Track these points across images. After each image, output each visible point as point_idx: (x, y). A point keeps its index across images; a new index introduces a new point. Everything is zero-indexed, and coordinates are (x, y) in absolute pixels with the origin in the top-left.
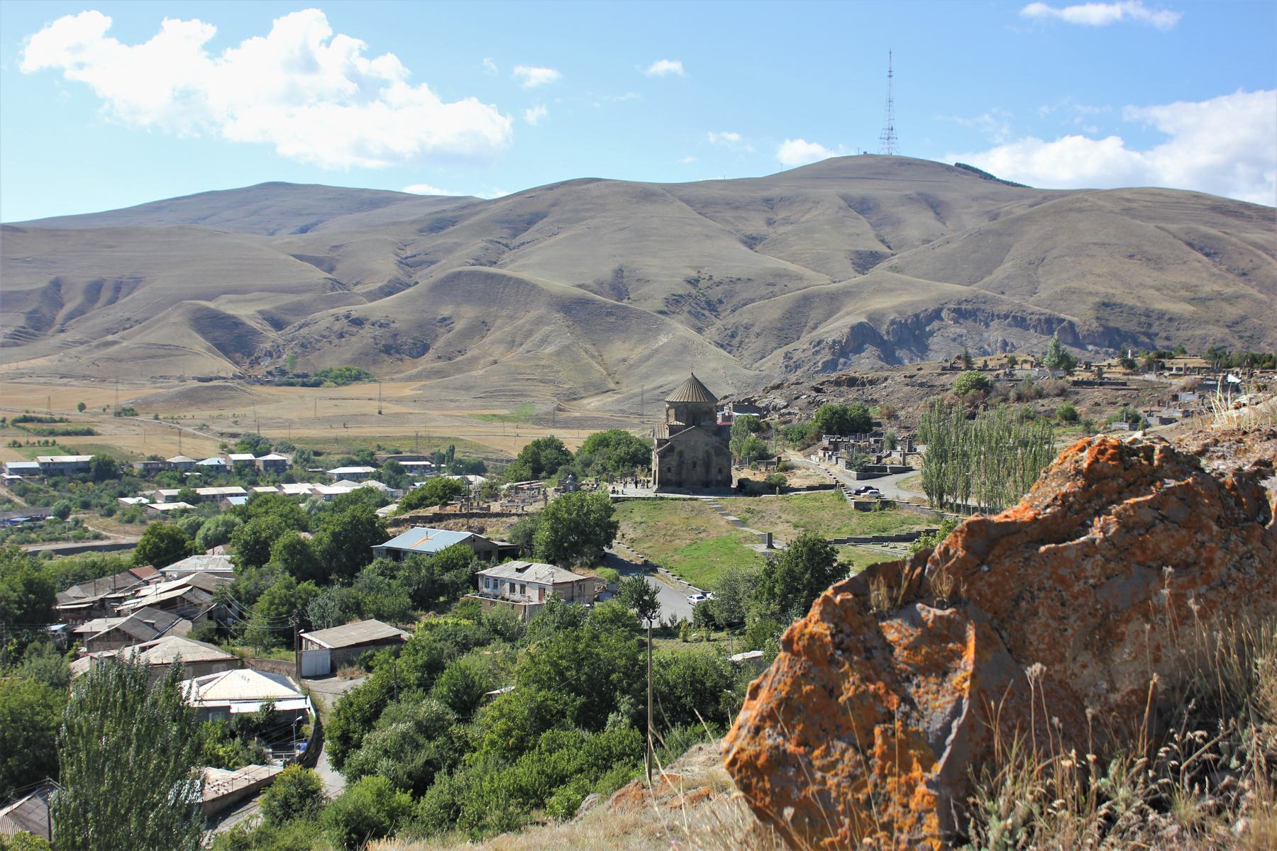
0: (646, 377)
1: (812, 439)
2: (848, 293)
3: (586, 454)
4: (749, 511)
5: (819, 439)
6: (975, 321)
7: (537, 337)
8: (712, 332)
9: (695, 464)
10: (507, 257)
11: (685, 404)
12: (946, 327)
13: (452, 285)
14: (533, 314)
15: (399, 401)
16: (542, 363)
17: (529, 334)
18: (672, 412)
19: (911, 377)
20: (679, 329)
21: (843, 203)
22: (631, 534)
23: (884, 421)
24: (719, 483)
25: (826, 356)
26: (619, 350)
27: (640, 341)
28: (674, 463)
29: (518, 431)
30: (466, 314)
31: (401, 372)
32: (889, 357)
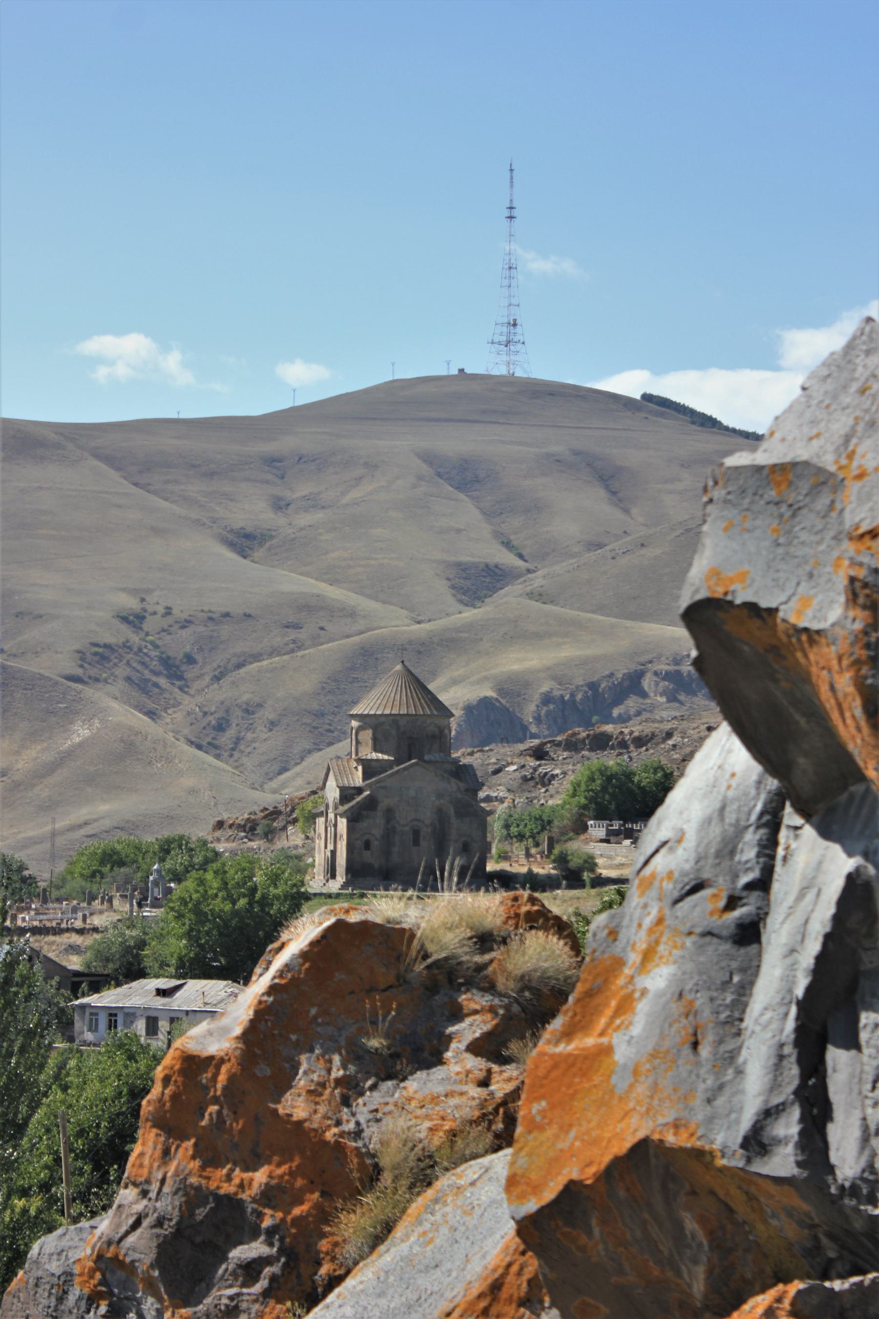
2: (452, 643)
9: (416, 833)
18: (367, 735)
20: (114, 710)
21: (425, 469)
28: (377, 832)
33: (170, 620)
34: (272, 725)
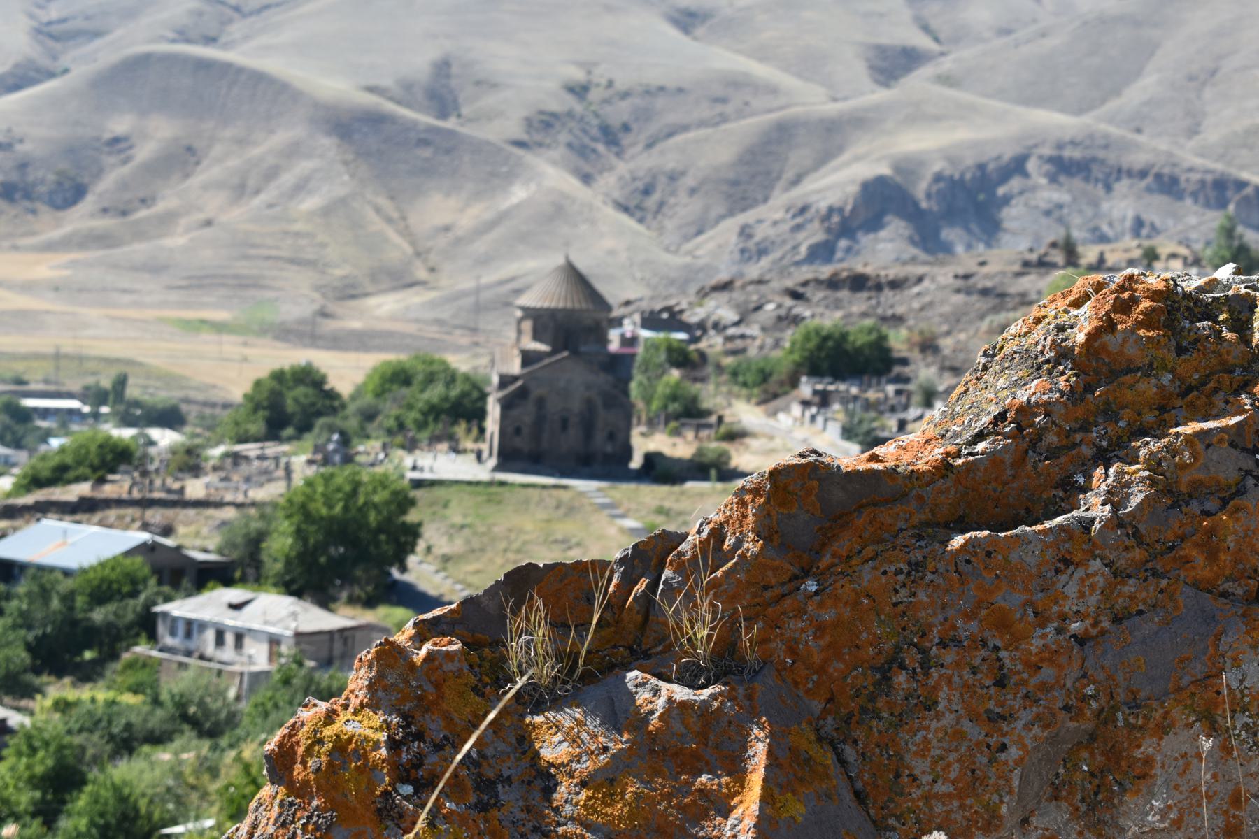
0: (485, 261)
1: (782, 383)
2: (859, 122)
3: (368, 399)
4: (660, 511)
5: (794, 383)
6: (1087, 179)
7: (287, 179)
8: (608, 182)
9: (564, 424)
10: (237, 29)
11: (552, 313)
12: (1034, 189)
13: (130, 78)
14: (282, 137)
15: (27, 287)
16: (298, 227)
17: (272, 174)
18: (527, 325)
19: (966, 277)
20: (549, 175)
22: (443, 546)
23: (915, 355)
24: (608, 458)
25: (814, 234)
26: (439, 209)
27: (477, 196)
29: (247, 351)
30: (158, 133)
31: (33, 233)
32: (929, 239)
33: (610, 92)
34: (693, 191)
